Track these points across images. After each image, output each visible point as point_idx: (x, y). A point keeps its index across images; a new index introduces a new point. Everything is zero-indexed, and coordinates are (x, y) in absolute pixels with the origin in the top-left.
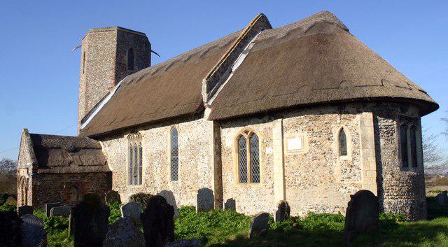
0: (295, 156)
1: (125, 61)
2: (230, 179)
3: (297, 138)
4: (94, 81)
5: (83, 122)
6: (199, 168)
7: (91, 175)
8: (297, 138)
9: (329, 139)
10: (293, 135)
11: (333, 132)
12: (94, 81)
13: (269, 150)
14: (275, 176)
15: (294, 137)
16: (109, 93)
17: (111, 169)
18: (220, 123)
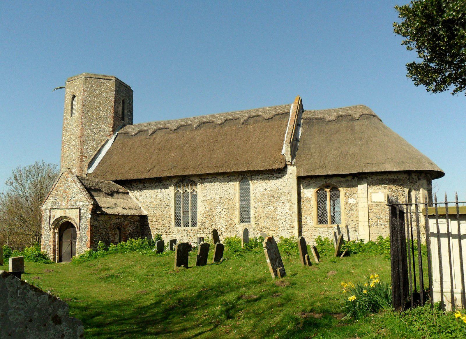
0: (377, 205)
1: (120, 111)
2: (309, 222)
3: (380, 193)
4: (90, 126)
5: (90, 165)
6: (278, 213)
7: (130, 217)
8: (380, 193)
9: (403, 195)
10: (377, 191)
11: (405, 190)
12: (90, 126)
13: (351, 201)
14: (360, 219)
15: (377, 192)
16: (107, 141)
17: (145, 212)
18: (301, 180)
